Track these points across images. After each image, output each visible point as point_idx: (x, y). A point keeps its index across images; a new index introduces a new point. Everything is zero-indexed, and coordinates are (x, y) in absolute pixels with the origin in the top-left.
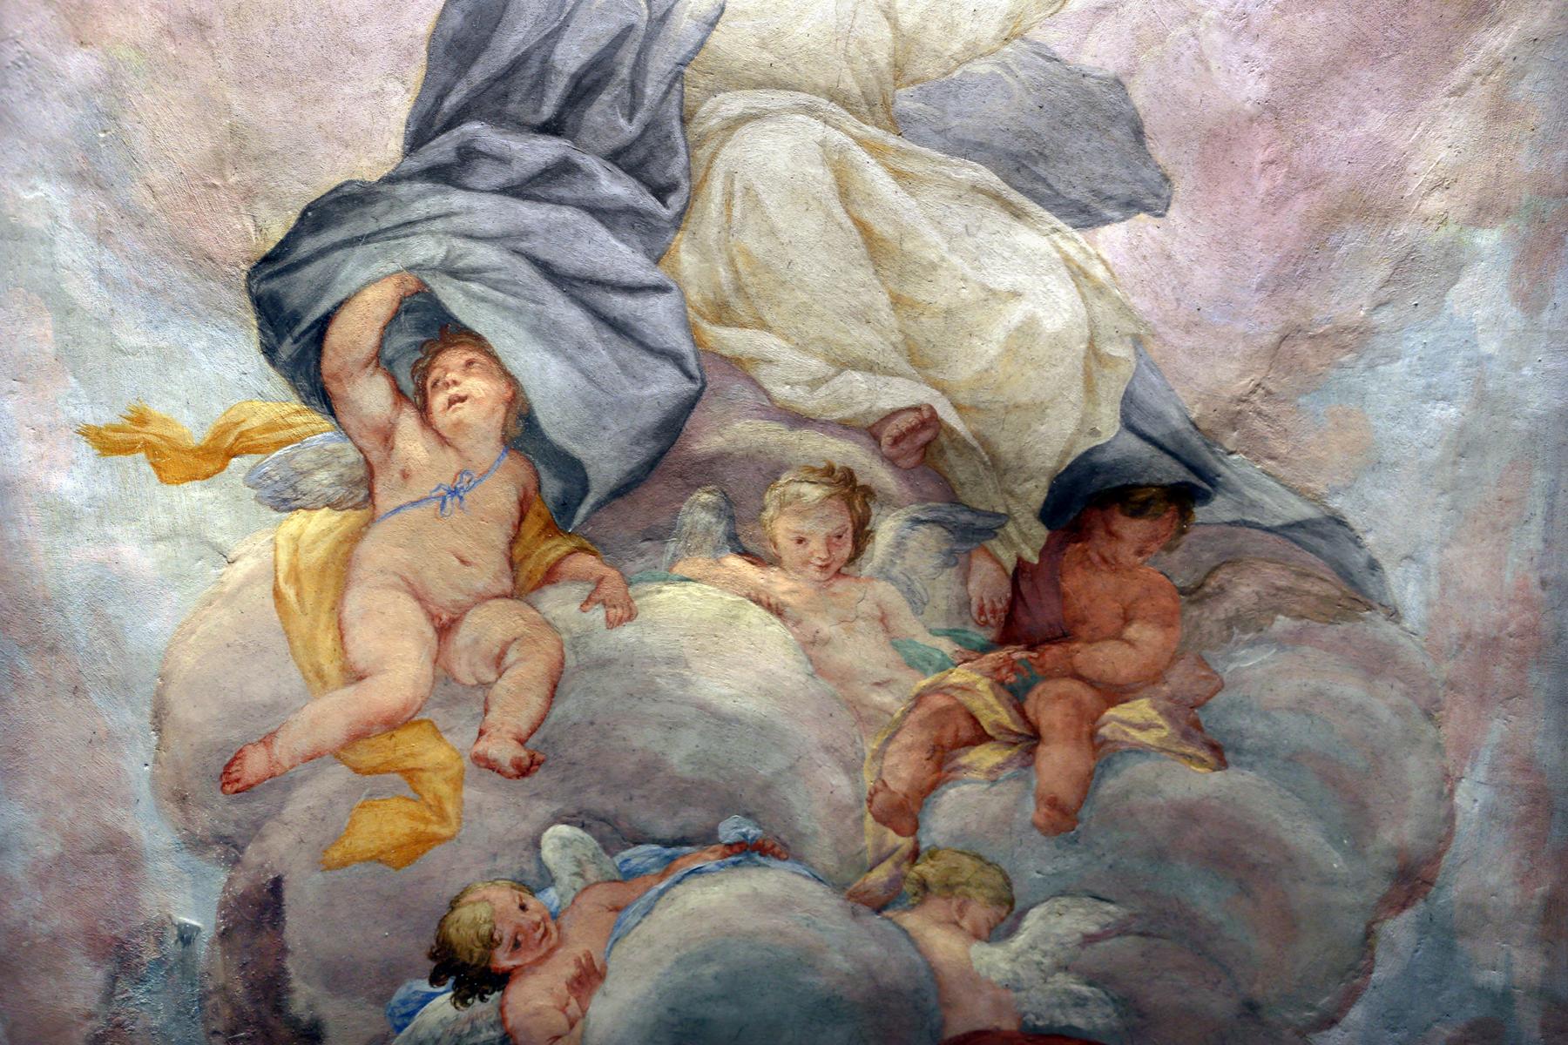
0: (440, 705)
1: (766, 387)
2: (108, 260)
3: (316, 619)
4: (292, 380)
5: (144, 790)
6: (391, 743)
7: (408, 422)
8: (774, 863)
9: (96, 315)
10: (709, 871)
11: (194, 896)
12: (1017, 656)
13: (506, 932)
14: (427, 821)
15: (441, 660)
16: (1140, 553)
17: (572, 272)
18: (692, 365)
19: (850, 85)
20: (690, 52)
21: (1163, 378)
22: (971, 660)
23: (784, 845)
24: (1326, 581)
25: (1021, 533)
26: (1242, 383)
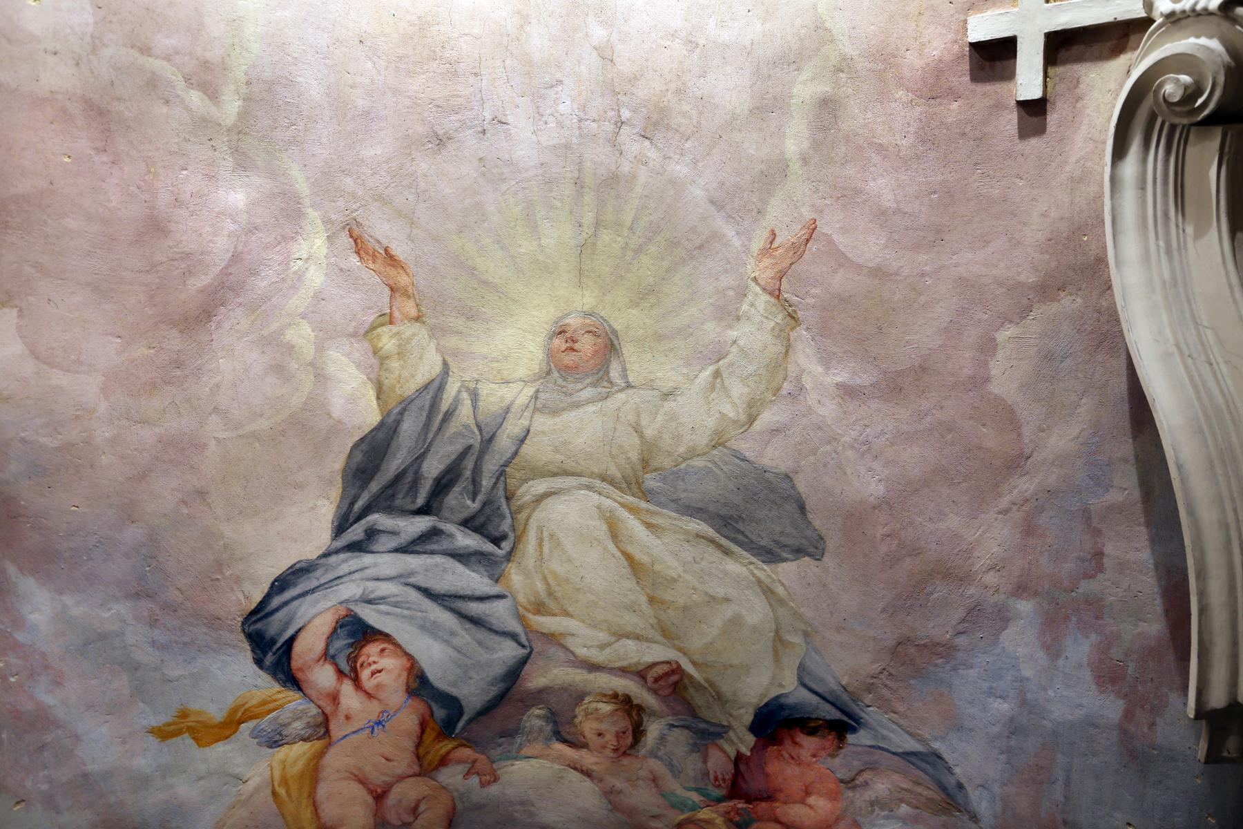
1: (571, 649)
2: (157, 635)
7: (347, 687)
9: (153, 666)
12: (740, 806)
16: (814, 756)
17: (442, 592)
18: (523, 639)
19: (614, 471)
20: (509, 458)
21: (823, 658)
22: (711, 806)
24: (932, 790)
25: (738, 737)
26: (874, 667)
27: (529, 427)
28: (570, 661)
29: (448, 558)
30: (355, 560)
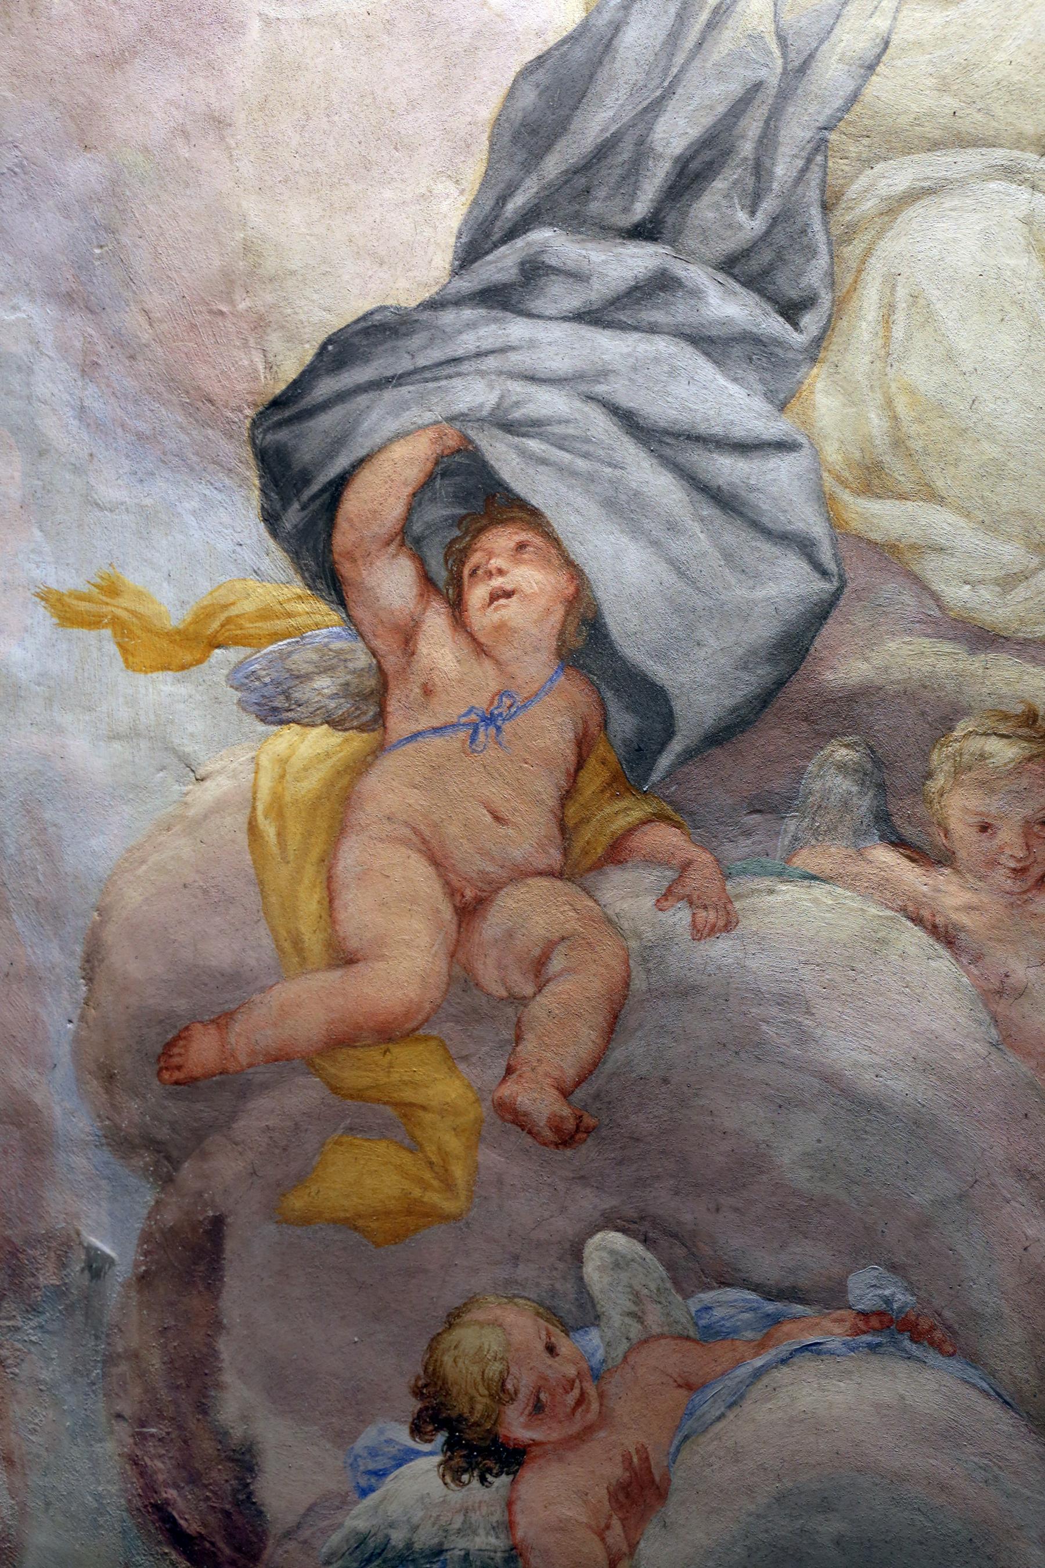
0: (456, 1019)
1: (935, 587)
2: (92, 395)
3: (299, 870)
4: (296, 557)
5: (63, 1052)
6: (385, 1061)
8: (933, 1357)
9: (73, 460)
10: (832, 1353)
11: (111, 1214)
13: (523, 1381)
14: (426, 1186)
15: (460, 955)
17: (662, 424)
18: (826, 555)
20: (838, 109)
23: (949, 1327)
27: (890, 33)
28: (927, 620)
29: (683, 344)
30: (493, 327)
